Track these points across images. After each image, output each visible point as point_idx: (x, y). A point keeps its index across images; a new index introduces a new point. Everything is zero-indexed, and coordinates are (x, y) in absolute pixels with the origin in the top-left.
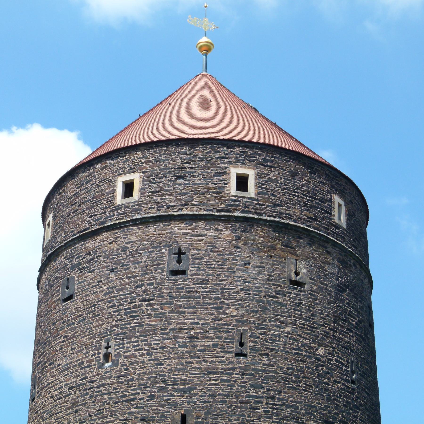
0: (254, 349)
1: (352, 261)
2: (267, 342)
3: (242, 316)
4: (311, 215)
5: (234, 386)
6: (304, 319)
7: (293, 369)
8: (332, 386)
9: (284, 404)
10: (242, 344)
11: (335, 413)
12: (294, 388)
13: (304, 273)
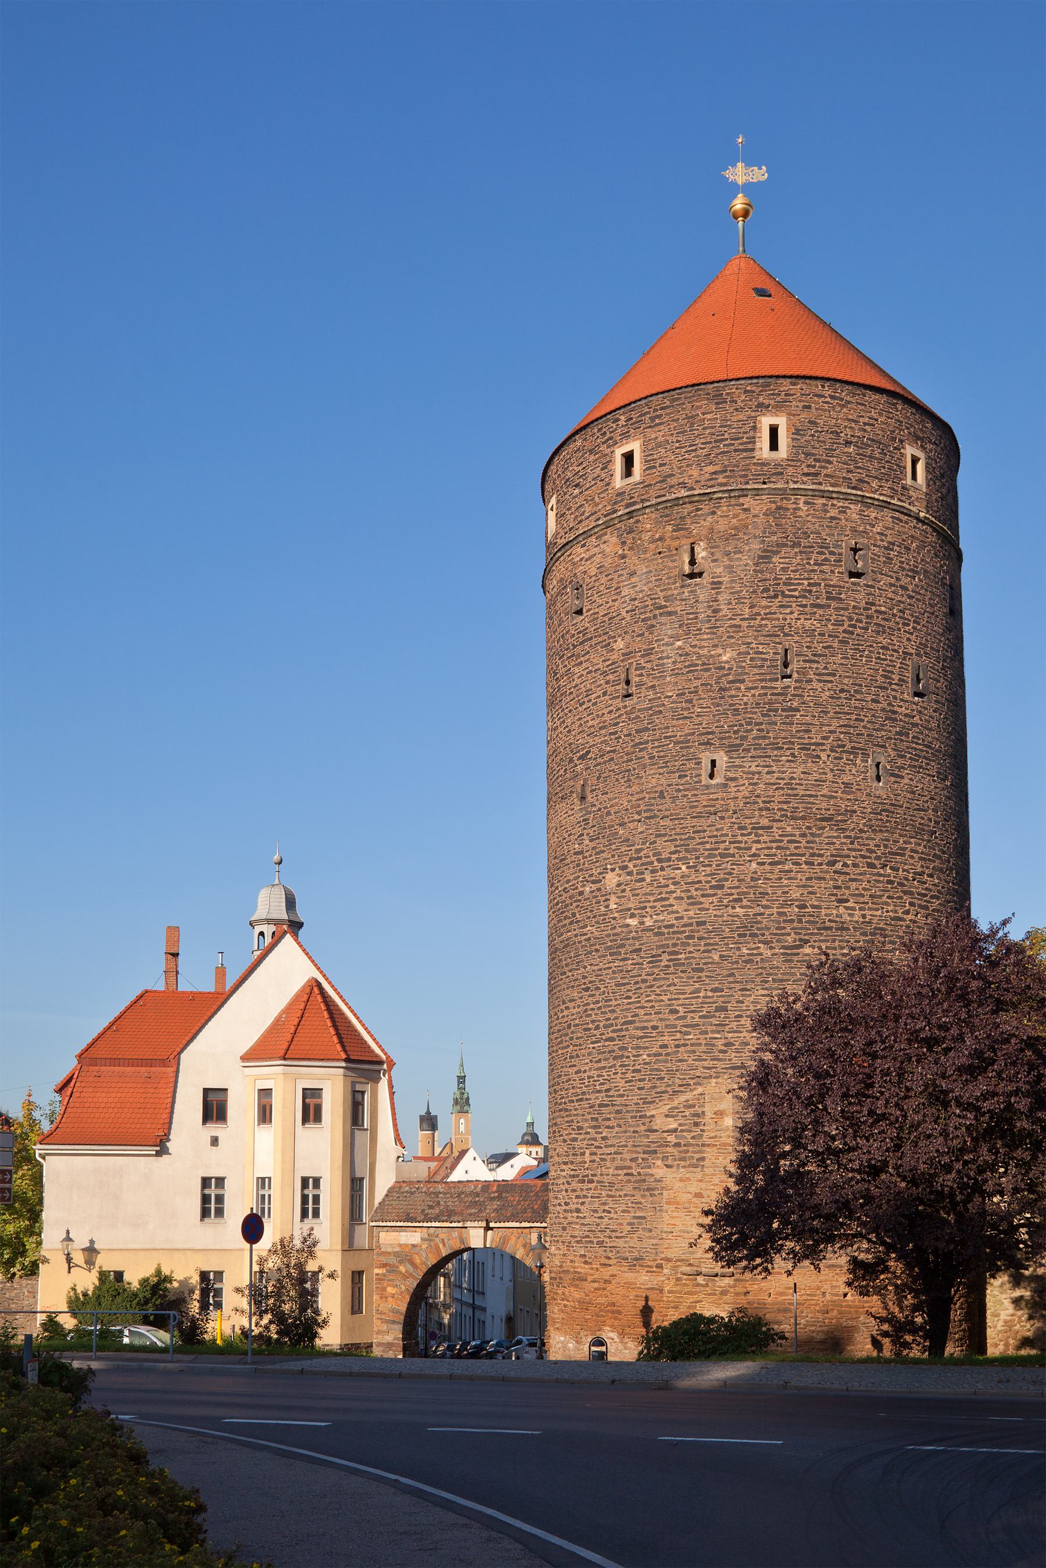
0: (639, 685)
2: (653, 670)
11: (747, 731)
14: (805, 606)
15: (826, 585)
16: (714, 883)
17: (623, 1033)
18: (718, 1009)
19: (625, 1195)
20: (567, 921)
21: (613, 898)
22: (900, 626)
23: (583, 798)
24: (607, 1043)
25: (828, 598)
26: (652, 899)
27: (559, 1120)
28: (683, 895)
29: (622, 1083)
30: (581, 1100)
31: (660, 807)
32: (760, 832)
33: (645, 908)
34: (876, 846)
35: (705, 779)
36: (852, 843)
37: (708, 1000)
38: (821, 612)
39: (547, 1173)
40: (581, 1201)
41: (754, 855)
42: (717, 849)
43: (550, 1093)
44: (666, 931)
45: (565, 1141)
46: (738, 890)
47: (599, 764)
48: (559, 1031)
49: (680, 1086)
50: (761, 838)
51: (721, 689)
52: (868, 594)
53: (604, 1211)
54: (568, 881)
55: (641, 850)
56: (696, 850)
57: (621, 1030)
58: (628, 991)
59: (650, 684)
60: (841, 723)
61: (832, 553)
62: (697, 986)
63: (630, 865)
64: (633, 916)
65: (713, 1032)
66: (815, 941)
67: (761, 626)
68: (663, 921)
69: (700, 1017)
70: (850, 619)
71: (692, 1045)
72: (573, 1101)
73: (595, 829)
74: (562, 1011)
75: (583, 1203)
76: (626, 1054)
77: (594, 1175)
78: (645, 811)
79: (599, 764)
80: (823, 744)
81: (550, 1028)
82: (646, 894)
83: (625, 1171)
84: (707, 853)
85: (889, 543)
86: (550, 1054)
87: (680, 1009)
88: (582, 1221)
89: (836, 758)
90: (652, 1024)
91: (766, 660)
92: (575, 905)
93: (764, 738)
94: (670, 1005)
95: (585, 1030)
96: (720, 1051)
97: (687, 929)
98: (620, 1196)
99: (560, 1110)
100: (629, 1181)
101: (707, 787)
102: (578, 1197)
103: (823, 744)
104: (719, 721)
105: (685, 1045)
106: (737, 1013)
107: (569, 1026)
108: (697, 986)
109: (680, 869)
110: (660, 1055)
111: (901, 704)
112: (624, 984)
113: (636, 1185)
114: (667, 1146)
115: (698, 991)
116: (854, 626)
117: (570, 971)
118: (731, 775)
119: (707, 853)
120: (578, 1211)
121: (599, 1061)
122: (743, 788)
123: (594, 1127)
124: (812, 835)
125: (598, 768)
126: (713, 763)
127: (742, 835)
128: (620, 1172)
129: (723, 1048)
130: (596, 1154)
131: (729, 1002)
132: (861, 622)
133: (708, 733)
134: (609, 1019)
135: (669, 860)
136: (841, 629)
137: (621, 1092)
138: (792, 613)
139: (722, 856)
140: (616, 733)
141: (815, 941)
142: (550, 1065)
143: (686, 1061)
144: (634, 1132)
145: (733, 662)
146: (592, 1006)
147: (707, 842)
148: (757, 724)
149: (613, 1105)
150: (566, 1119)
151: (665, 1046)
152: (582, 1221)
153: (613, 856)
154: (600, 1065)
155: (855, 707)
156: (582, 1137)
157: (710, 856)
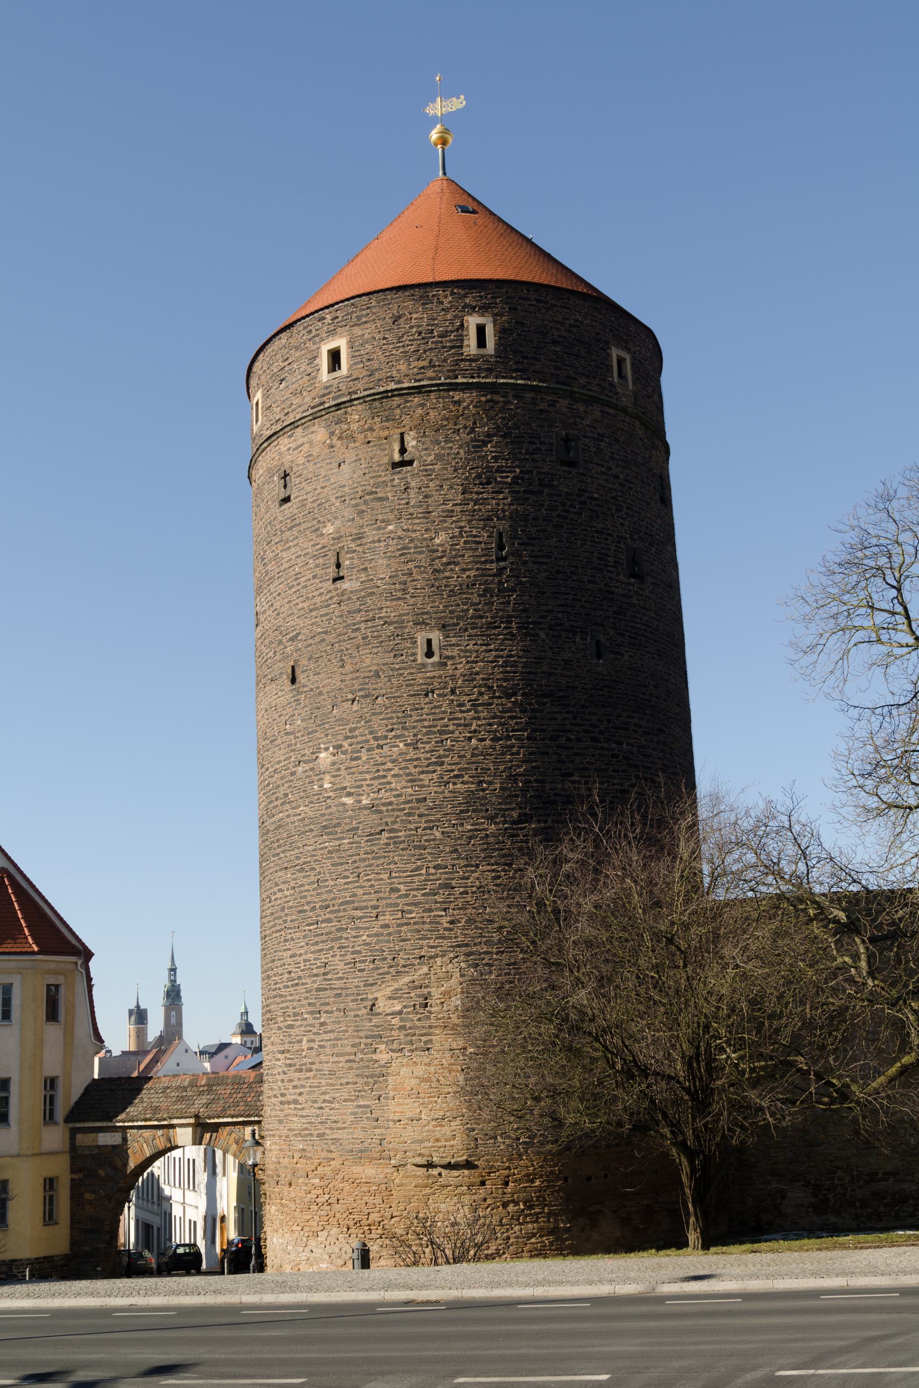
0: (351, 568)
1: (511, 395)
3: (338, 530)
4: (425, 363)
5: (332, 619)
6: (413, 506)
7: (397, 576)
8: (458, 577)
9: (386, 622)
10: (338, 566)
11: (463, 611)
12: (399, 599)
13: (413, 447)
14: (518, 492)
15: (538, 473)
16: (433, 760)
17: (342, 914)
18: (441, 886)
19: (347, 1083)
20: (279, 802)
21: (327, 778)
22: (614, 512)
23: (293, 680)
24: (323, 925)
25: (540, 485)
26: (368, 776)
27: (272, 1007)
28: (401, 772)
29: (341, 966)
30: (297, 984)
31: (375, 686)
32: (480, 708)
33: (362, 786)
34: (598, 721)
35: (420, 658)
36: (575, 718)
37: (432, 877)
38: (533, 498)
39: (261, 1063)
40: (298, 1091)
41: (475, 731)
42: (435, 726)
43: (263, 979)
44: (384, 809)
45: (280, 1028)
46: (459, 766)
47: (310, 645)
48: (272, 914)
49: (404, 966)
50: (482, 715)
51: (435, 570)
52: (580, 482)
53: (324, 1101)
54: (279, 762)
55: (354, 729)
56: (414, 728)
57: (339, 911)
58: (346, 870)
59: (363, 567)
60: (558, 602)
61: (542, 443)
62: (419, 863)
63: (345, 744)
64: (349, 795)
65: (437, 909)
66: (540, 815)
67: (474, 510)
68: (381, 798)
69: (423, 895)
70: (564, 504)
71: (415, 923)
72: (287, 987)
73: (308, 709)
74: (275, 894)
75: (300, 1094)
76: (345, 935)
77: (313, 1063)
78: (360, 690)
79: (310, 645)
80: (541, 623)
81: (263, 911)
82: (361, 773)
83: (347, 1058)
84: (425, 730)
85: (599, 434)
86: (262, 938)
87: (401, 887)
88: (300, 1113)
89: (554, 636)
90: (372, 903)
91: (480, 543)
92: (287, 785)
93: (481, 617)
94: (391, 884)
95: (300, 912)
96: (445, 929)
97: (407, 806)
98: (341, 1084)
99: (275, 997)
100: (351, 1068)
101: (424, 665)
102: (295, 1087)
103: (541, 623)
104: (434, 602)
105: (407, 924)
106: (462, 890)
107: (283, 909)
108: (419, 863)
109: (398, 746)
110: (382, 935)
111: (618, 584)
112: (342, 864)
113: (358, 1072)
114: (392, 1030)
115: (419, 868)
116: (568, 511)
117: (283, 852)
118: (449, 653)
119: (425, 730)
120: (296, 1102)
121: (317, 943)
122: (461, 666)
123: (312, 1013)
124: (534, 710)
125: (310, 648)
126: (429, 642)
127: (462, 712)
128: (342, 1059)
129: (448, 925)
130: (314, 1041)
131: (453, 879)
132: (575, 507)
133: (423, 613)
134: (326, 900)
135: (386, 737)
136: (555, 514)
137: (340, 975)
138: (504, 498)
139: (441, 732)
140: (327, 614)
141: (540, 815)
142: (263, 950)
143: (409, 940)
144: (356, 1016)
145: (446, 545)
146: (306, 887)
147: (426, 720)
148: (473, 604)
149: (331, 989)
150: (281, 1005)
151: (387, 926)
152: (300, 1113)
153: (327, 735)
154: (317, 948)
155: (572, 588)
156: (299, 1023)
157: (427, 733)
